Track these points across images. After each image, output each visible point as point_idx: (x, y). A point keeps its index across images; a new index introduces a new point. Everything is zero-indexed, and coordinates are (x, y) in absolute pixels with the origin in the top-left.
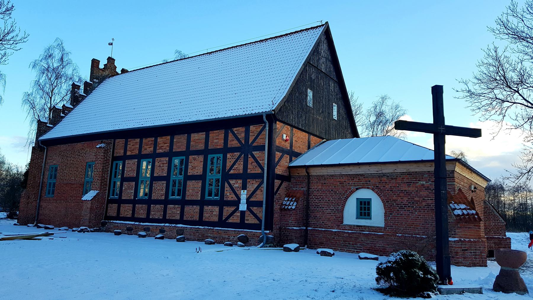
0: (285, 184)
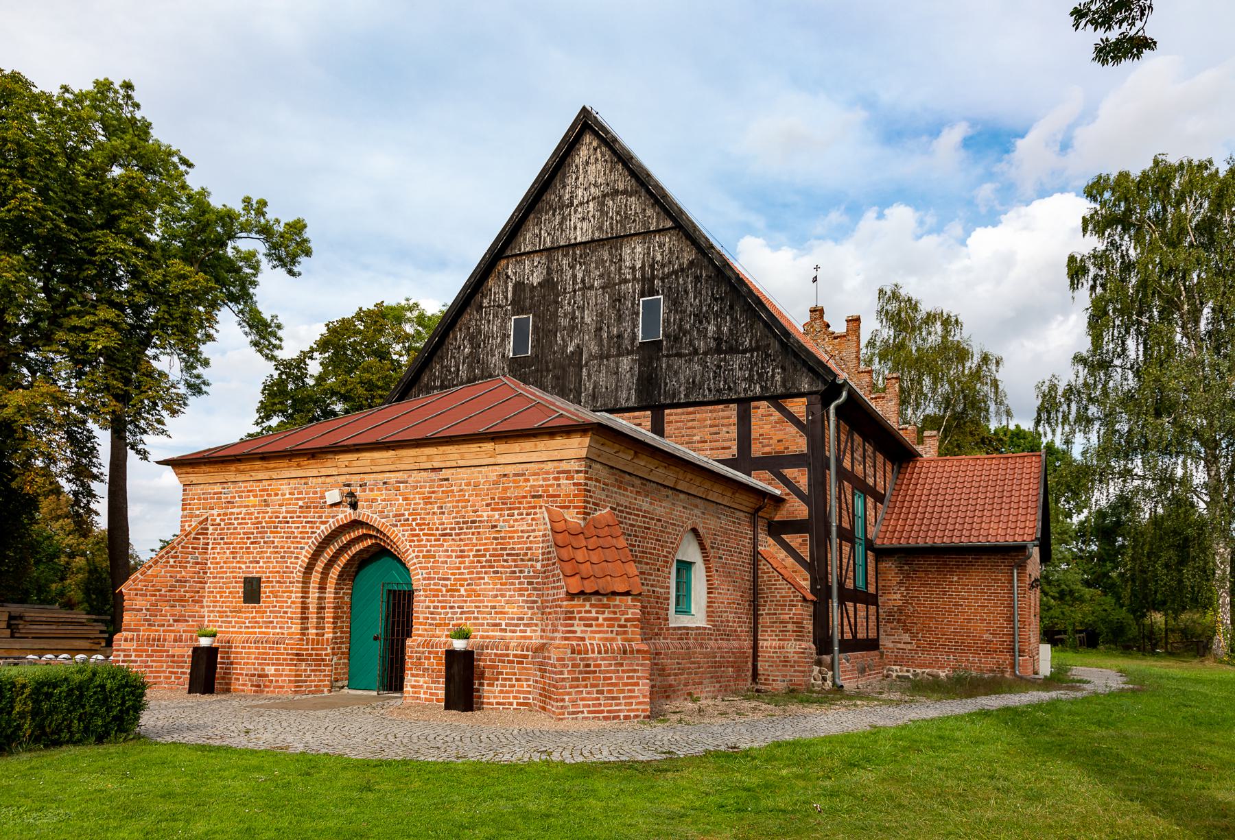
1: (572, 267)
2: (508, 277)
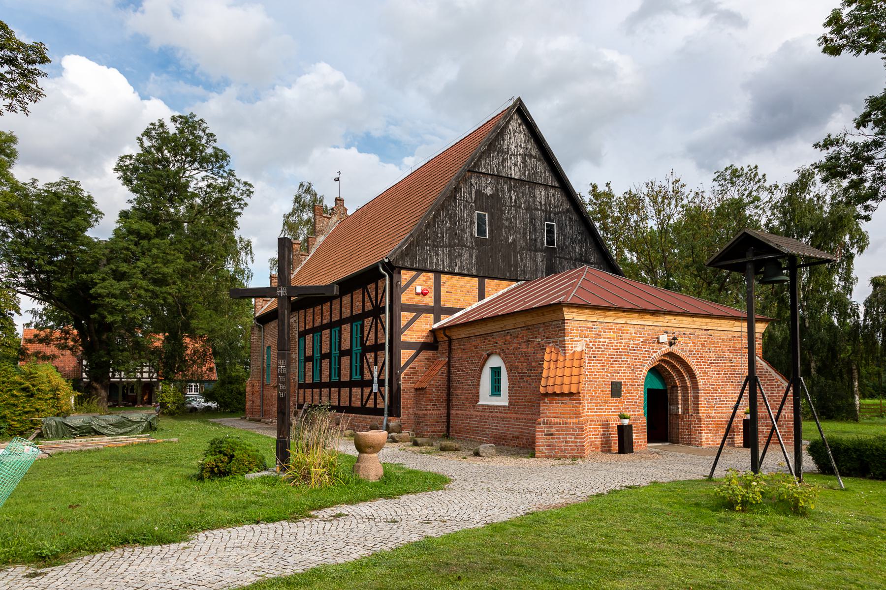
0: (424, 354)
1: (509, 191)
2: (472, 184)
